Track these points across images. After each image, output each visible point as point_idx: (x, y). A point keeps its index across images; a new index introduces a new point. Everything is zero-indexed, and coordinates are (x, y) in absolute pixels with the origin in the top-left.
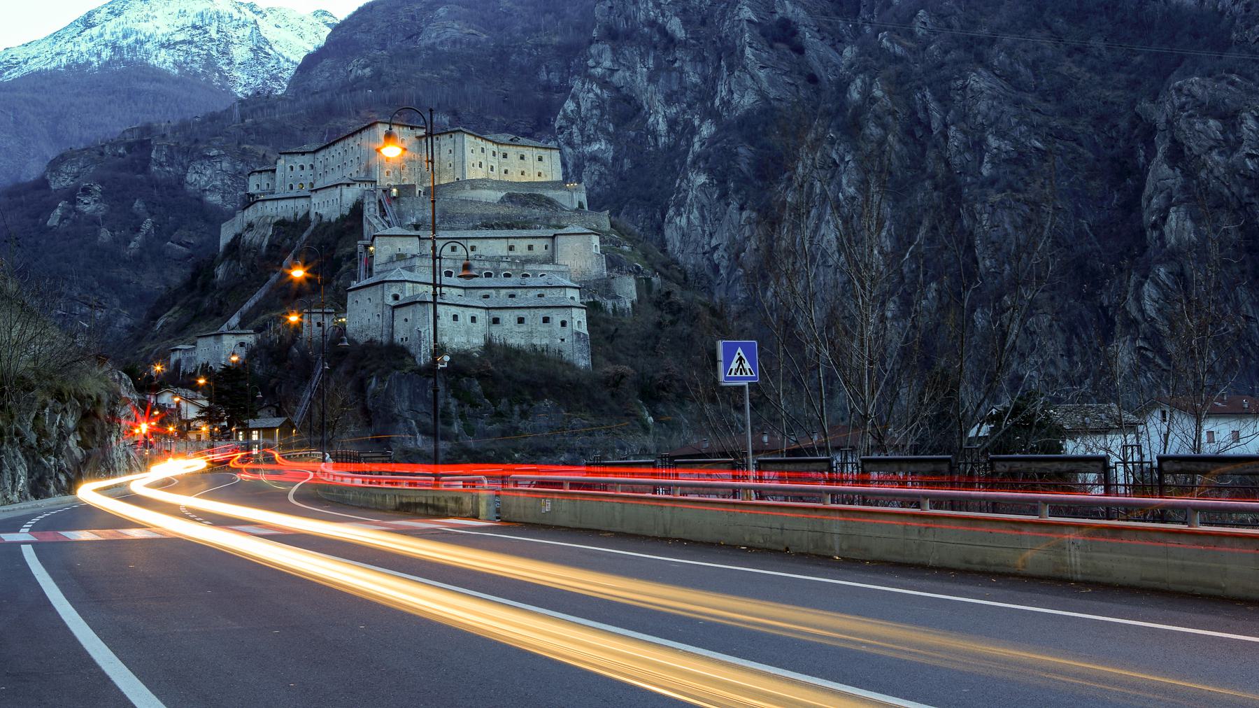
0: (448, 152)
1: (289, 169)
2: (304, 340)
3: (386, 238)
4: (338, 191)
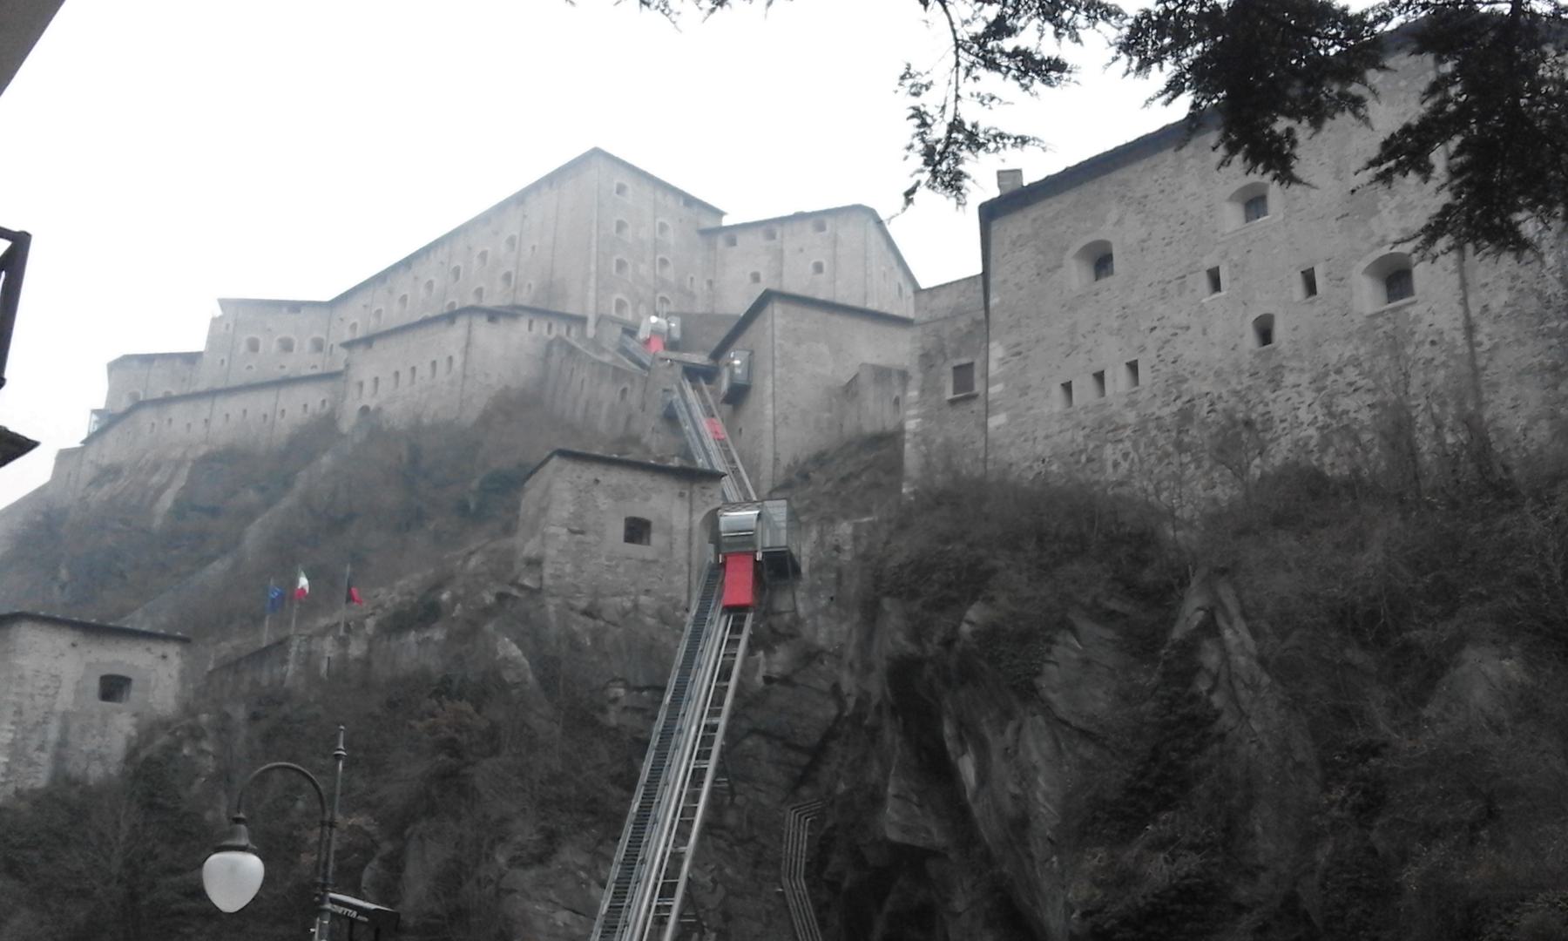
0: (810, 268)
1: (243, 348)
2: (552, 605)
3: (817, 315)
4: (458, 331)
